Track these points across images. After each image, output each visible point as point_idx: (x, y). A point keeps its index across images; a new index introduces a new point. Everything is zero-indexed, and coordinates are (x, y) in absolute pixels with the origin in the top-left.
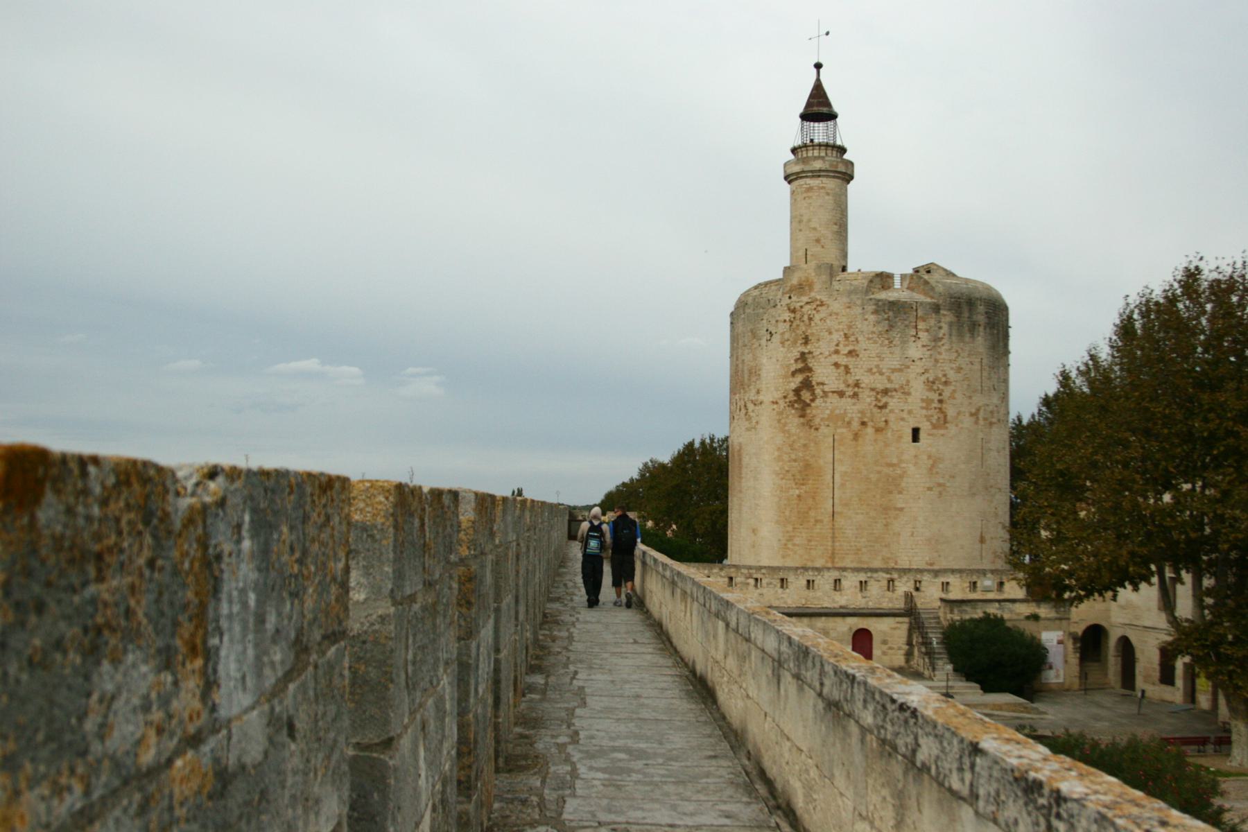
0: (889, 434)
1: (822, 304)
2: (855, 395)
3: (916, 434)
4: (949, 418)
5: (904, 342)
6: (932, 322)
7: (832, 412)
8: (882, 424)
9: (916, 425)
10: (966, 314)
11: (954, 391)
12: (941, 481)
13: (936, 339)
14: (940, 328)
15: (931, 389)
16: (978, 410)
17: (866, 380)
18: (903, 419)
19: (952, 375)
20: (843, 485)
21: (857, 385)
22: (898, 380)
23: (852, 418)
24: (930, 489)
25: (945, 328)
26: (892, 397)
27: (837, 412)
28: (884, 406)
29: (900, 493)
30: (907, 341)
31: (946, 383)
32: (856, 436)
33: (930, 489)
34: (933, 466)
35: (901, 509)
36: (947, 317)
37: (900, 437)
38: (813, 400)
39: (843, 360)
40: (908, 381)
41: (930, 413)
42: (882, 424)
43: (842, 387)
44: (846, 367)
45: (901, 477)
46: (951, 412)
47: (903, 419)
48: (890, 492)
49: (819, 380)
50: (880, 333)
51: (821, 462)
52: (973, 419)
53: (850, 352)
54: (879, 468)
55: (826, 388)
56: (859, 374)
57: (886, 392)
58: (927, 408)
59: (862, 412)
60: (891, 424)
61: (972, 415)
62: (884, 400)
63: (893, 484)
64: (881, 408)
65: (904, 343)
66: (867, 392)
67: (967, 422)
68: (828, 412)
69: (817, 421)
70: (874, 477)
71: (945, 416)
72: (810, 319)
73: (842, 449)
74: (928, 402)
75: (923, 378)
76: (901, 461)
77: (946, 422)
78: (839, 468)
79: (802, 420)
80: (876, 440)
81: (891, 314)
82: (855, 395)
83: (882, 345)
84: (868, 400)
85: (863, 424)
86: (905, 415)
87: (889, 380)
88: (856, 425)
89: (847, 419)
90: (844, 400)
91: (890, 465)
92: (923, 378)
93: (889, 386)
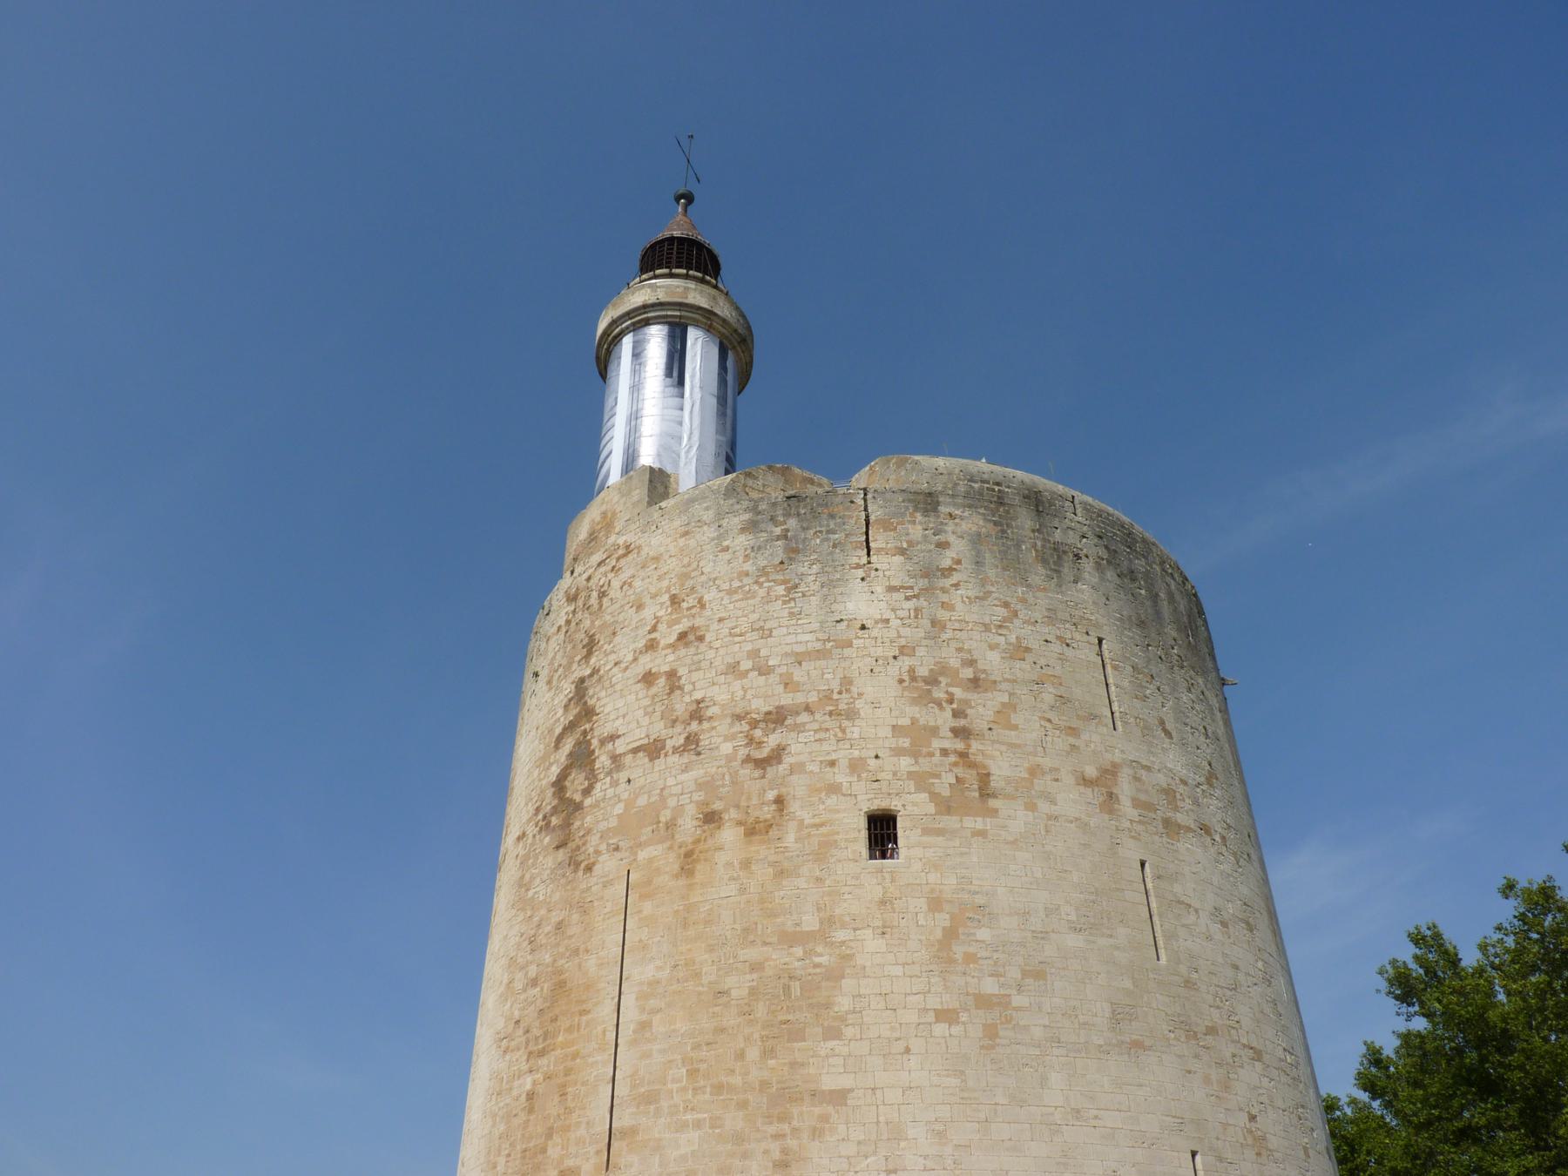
0: (790, 839)
1: (628, 549)
2: (692, 742)
3: (882, 832)
4: (996, 783)
5: (829, 584)
6: (916, 532)
7: (629, 804)
8: (768, 812)
9: (879, 804)
10: (1025, 521)
11: (1010, 707)
12: (990, 987)
13: (930, 572)
14: (943, 545)
15: (924, 698)
16: (1109, 773)
17: (720, 694)
18: (834, 789)
19: (992, 661)
20: (644, 1026)
21: (697, 714)
22: (818, 678)
23: (679, 810)
24: (945, 1016)
25: (959, 548)
26: (799, 728)
27: (642, 801)
28: (777, 755)
29: (833, 1033)
30: (843, 581)
31: (975, 683)
32: (689, 861)
33: (945, 1016)
34: (950, 934)
35: (839, 1097)
36: (972, 522)
37: (828, 844)
38: (587, 792)
39: (661, 662)
40: (847, 683)
41: (925, 765)
42: (768, 812)
43: (659, 729)
44: (672, 675)
45: (834, 976)
46: (1002, 768)
47: (834, 789)
48: (797, 1035)
49: (606, 730)
50: (763, 572)
51: (591, 963)
52: (1094, 796)
53: (682, 636)
54: (752, 954)
55: (621, 746)
56: (703, 684)
57: (777, 718)
58: (915, 754)
59: (706, 785)
60: (794, 807)
61: (1085, 781)
62: (773, 740)
63: (796, 1005)
64: (761, 764)
65: (830, 586)
66: (723, 726)
67: (1071, 801)
68: (619, 809)
69: (594, 840)
70: (738, 985)
71: (985, 778)
72: (602, 595)
73: (648, 907)
74: (916, 738)
75: (894, 670)
76: (829, 922)
77: (986, 792)
78: (639, 972)
79: (561, 855)
80: (746, 864)
81: (792, 523)
82: (692, 742)
83: (768, 600)
84: (727, 748)
85: (711, 818)
86: (841, 776)
87: (788, 684)
88: (689, 825)
89: (665, 816)
90: (660, 763)
91: (791, 939)
92: (894, 670)
93: (787, 700)
